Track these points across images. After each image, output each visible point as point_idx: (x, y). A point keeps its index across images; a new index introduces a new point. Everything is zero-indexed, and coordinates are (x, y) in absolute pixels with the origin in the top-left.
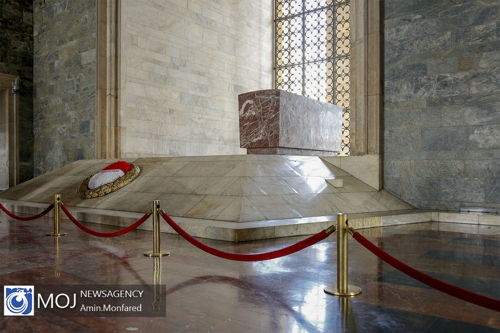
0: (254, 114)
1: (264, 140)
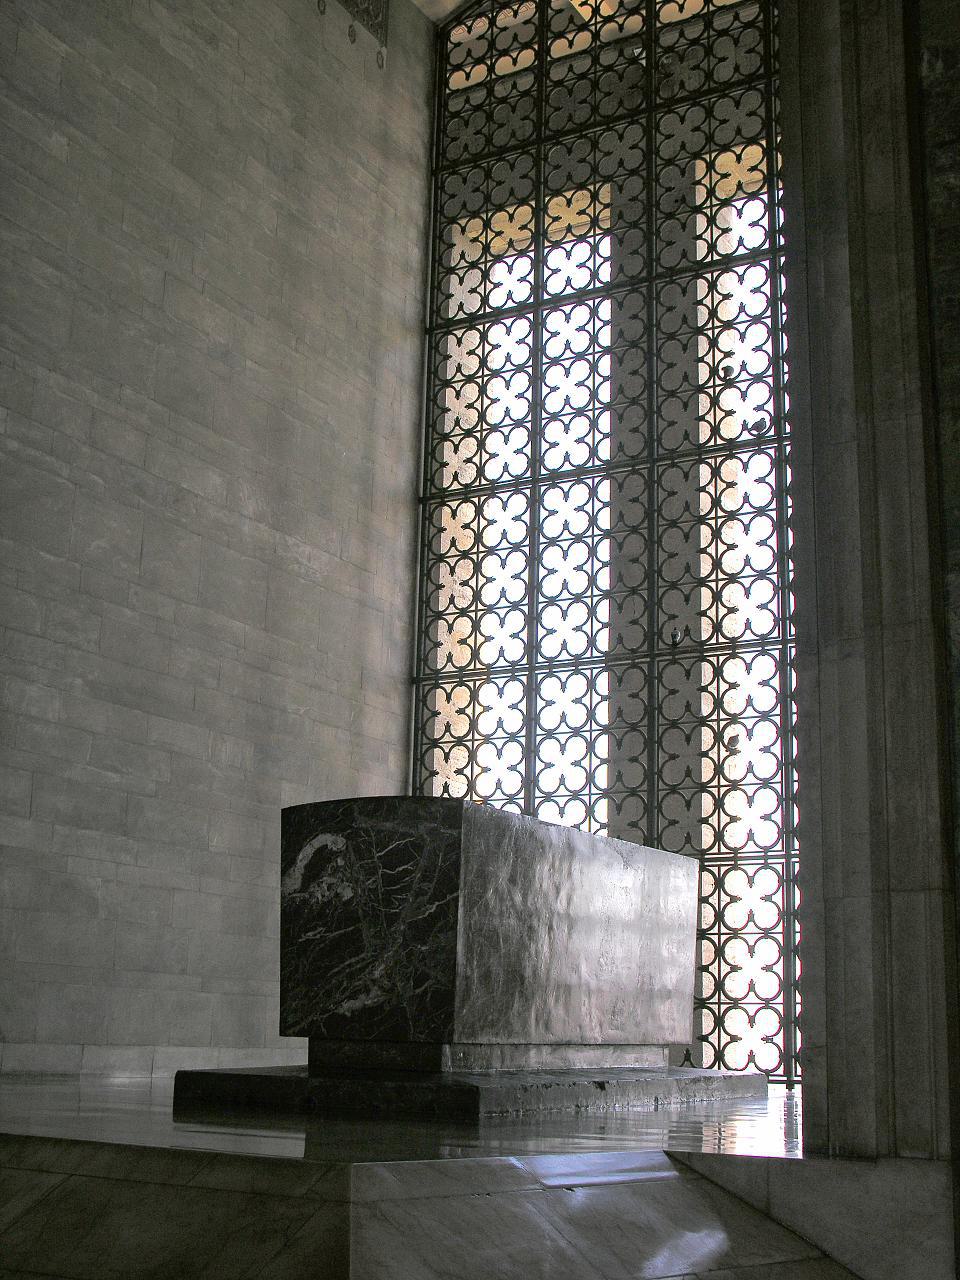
0: (348, 894)
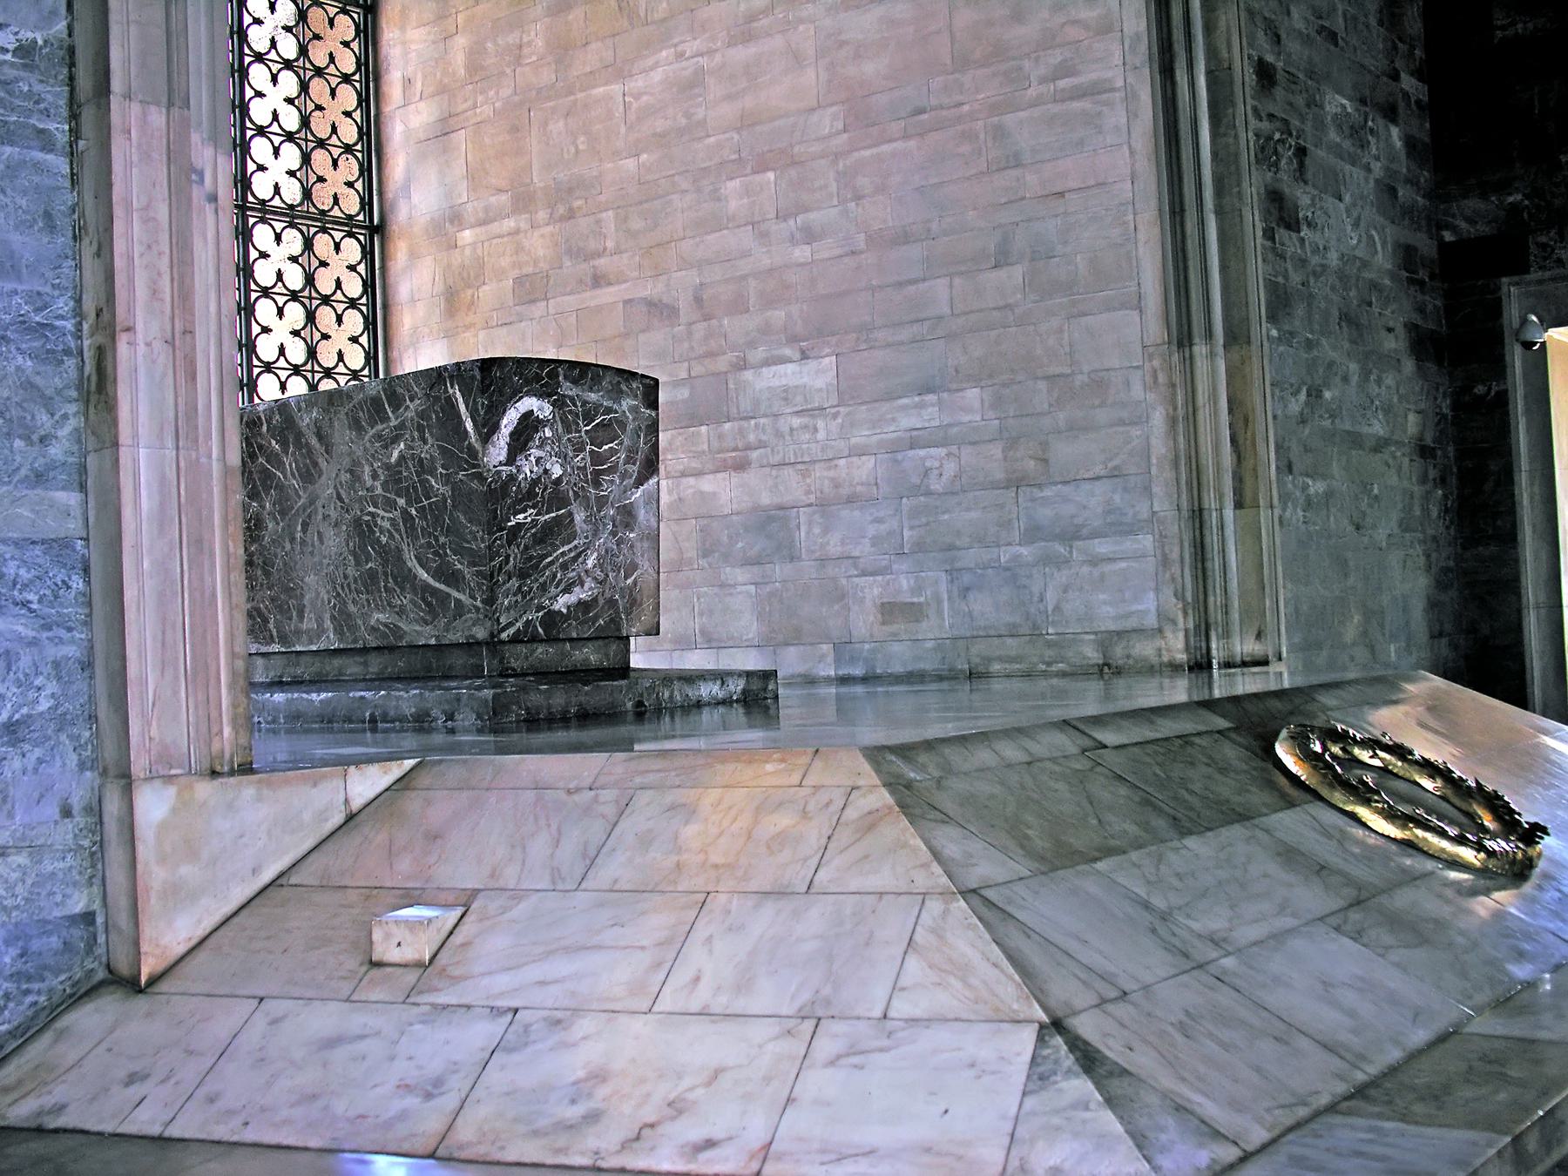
0: (557, 471)
1: (601, 601)
